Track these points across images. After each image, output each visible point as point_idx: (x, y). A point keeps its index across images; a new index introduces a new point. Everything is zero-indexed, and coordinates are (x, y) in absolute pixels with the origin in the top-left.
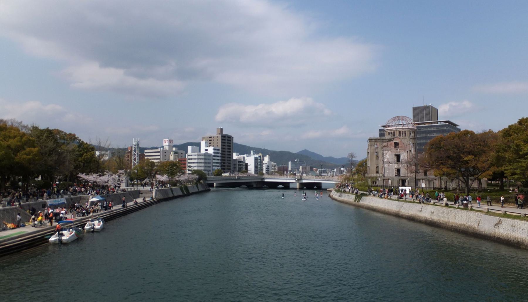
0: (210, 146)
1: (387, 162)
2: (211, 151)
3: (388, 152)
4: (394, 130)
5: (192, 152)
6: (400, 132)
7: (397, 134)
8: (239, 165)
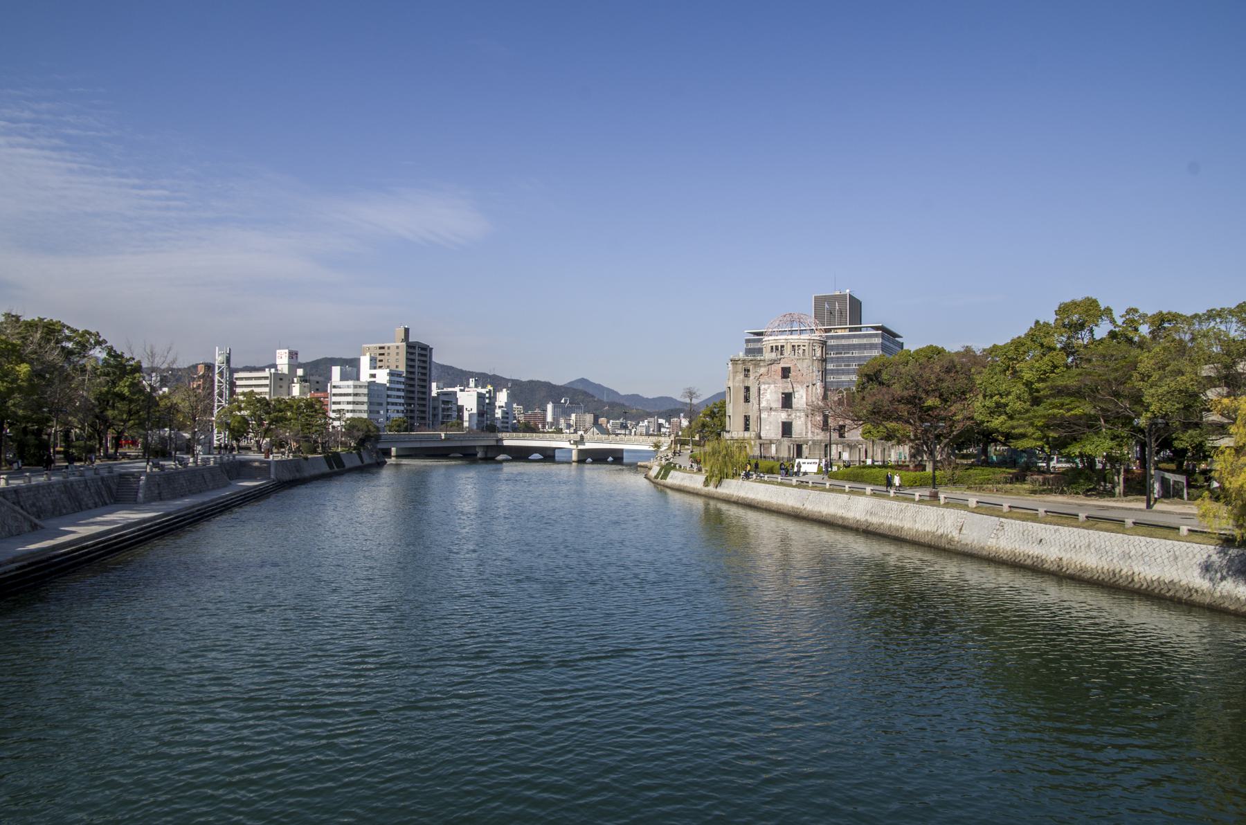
0: (380, 367)
2: (382, 377)
5: (342, 379)
6: (793, 346)
7: (788, 350)
8: (444, 410)
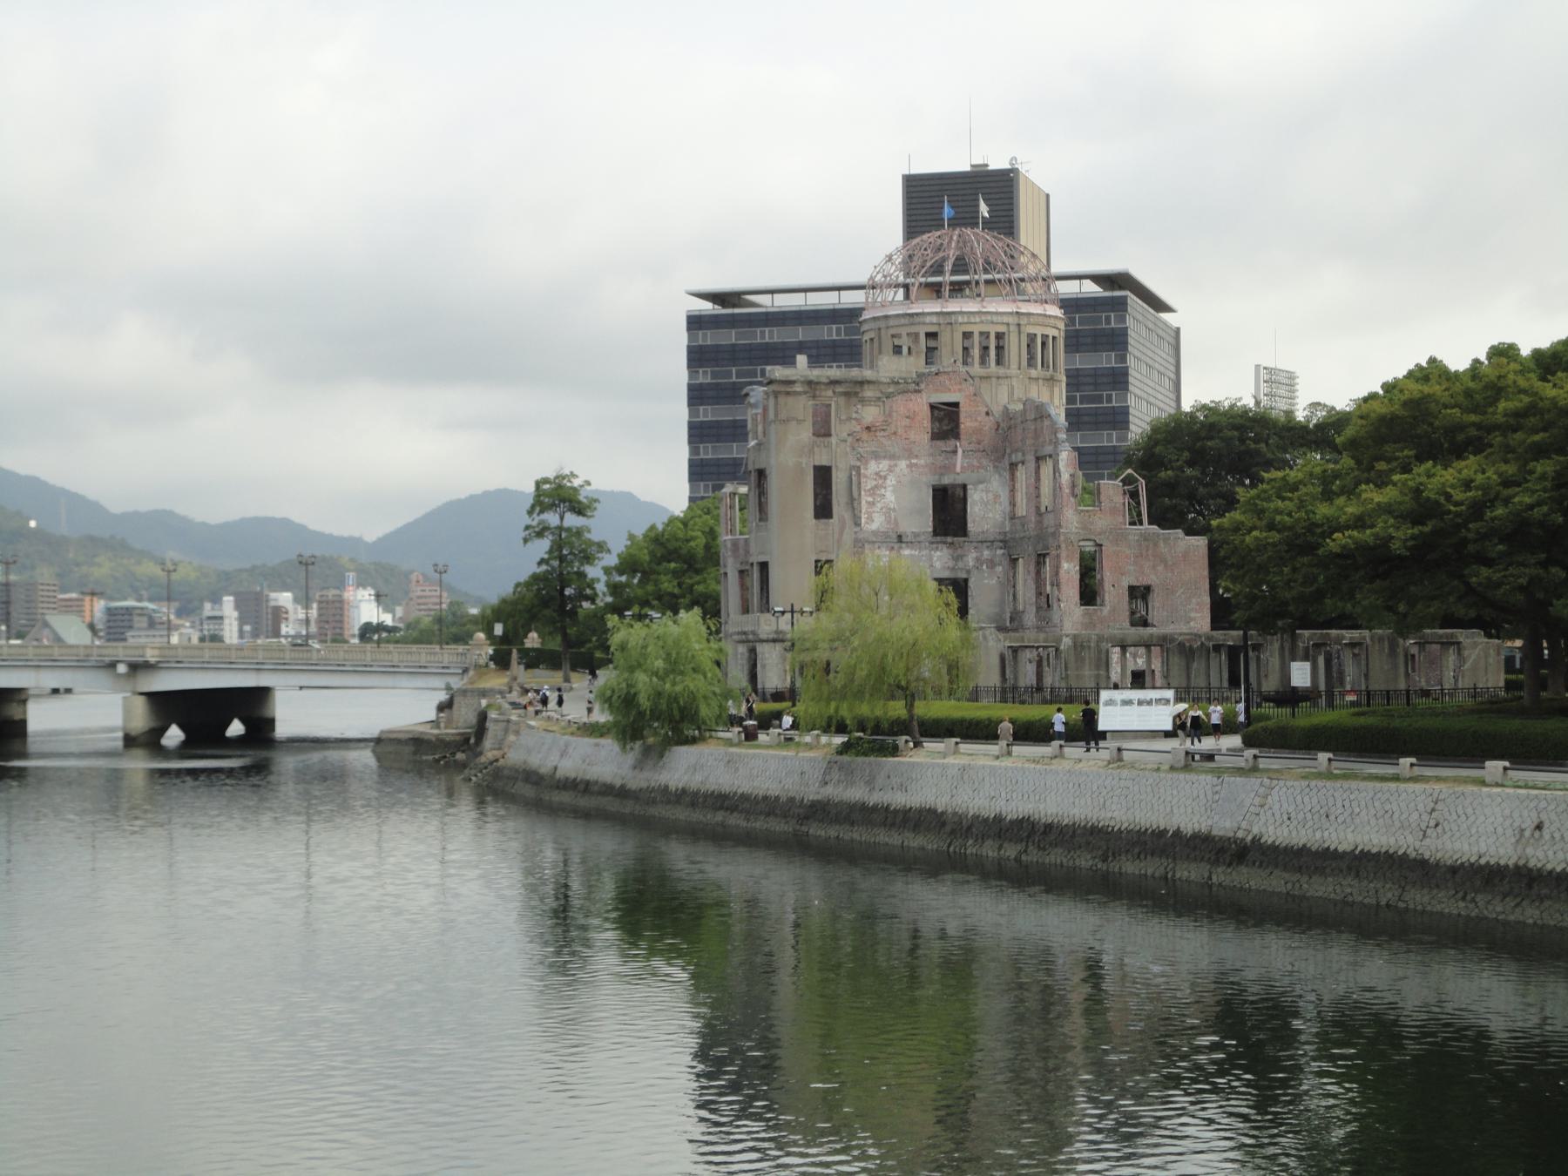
1: (886, 534)
3: (891, 470)
4: (928, 319)
6: (967, 335)
7: (950, 345)
